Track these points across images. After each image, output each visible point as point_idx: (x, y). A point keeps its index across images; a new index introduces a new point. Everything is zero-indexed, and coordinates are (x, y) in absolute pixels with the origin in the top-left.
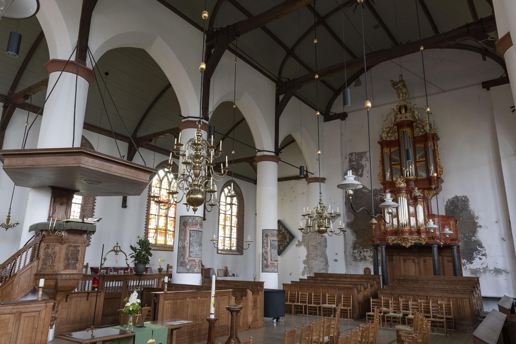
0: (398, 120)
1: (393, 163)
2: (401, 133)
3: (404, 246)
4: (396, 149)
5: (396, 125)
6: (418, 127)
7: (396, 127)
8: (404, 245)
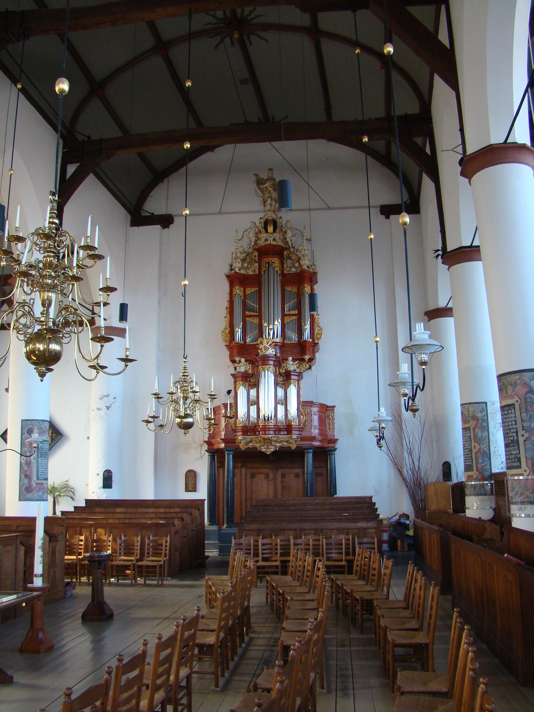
0: (261, 243)
1: (247, 313)
2: (264, 264)
3: (264, 452)
4: (253, 290)
5: (256, 250)
6: (290, 258)
7: (256, 253)
8: (264, 450)
